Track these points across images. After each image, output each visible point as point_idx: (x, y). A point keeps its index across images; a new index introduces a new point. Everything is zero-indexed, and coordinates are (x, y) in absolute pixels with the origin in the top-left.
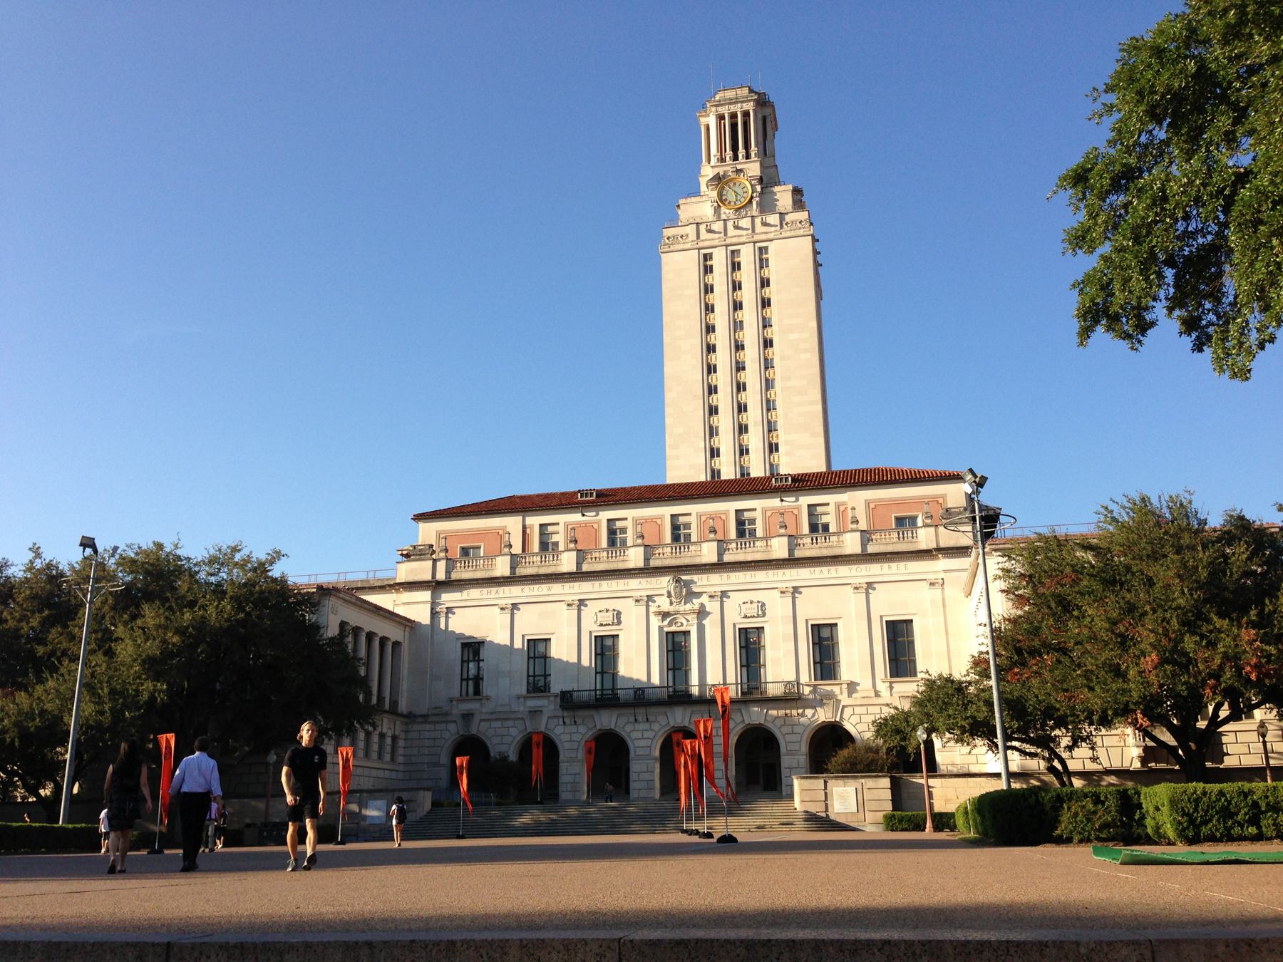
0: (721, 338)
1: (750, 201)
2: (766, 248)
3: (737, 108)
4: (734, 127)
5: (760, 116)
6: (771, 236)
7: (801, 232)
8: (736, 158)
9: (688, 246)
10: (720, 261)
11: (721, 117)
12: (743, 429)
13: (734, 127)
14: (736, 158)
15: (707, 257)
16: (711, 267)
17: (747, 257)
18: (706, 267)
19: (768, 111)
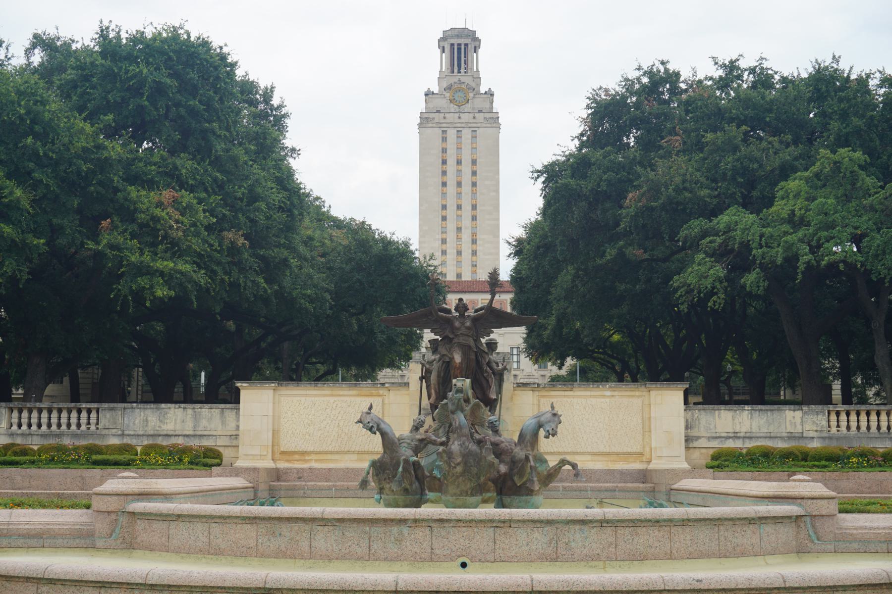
0: (451, 179)
1: (468, 102)
2: (476, 131)
3: (463, 41)
4: (459, 49)
5: (473, 46)
6: (479, 125)
7: (494, 125)
8: (459, 72)
9: (434, 125)
10: (452, 134)
11: (452, 45)
12: (459, 229)
13: (459, 49)
14: (459, 72)
15: (444, 132)
16: (446, 138)
17: (467, 134)
18: (443, 138)
19: (478, 43)
